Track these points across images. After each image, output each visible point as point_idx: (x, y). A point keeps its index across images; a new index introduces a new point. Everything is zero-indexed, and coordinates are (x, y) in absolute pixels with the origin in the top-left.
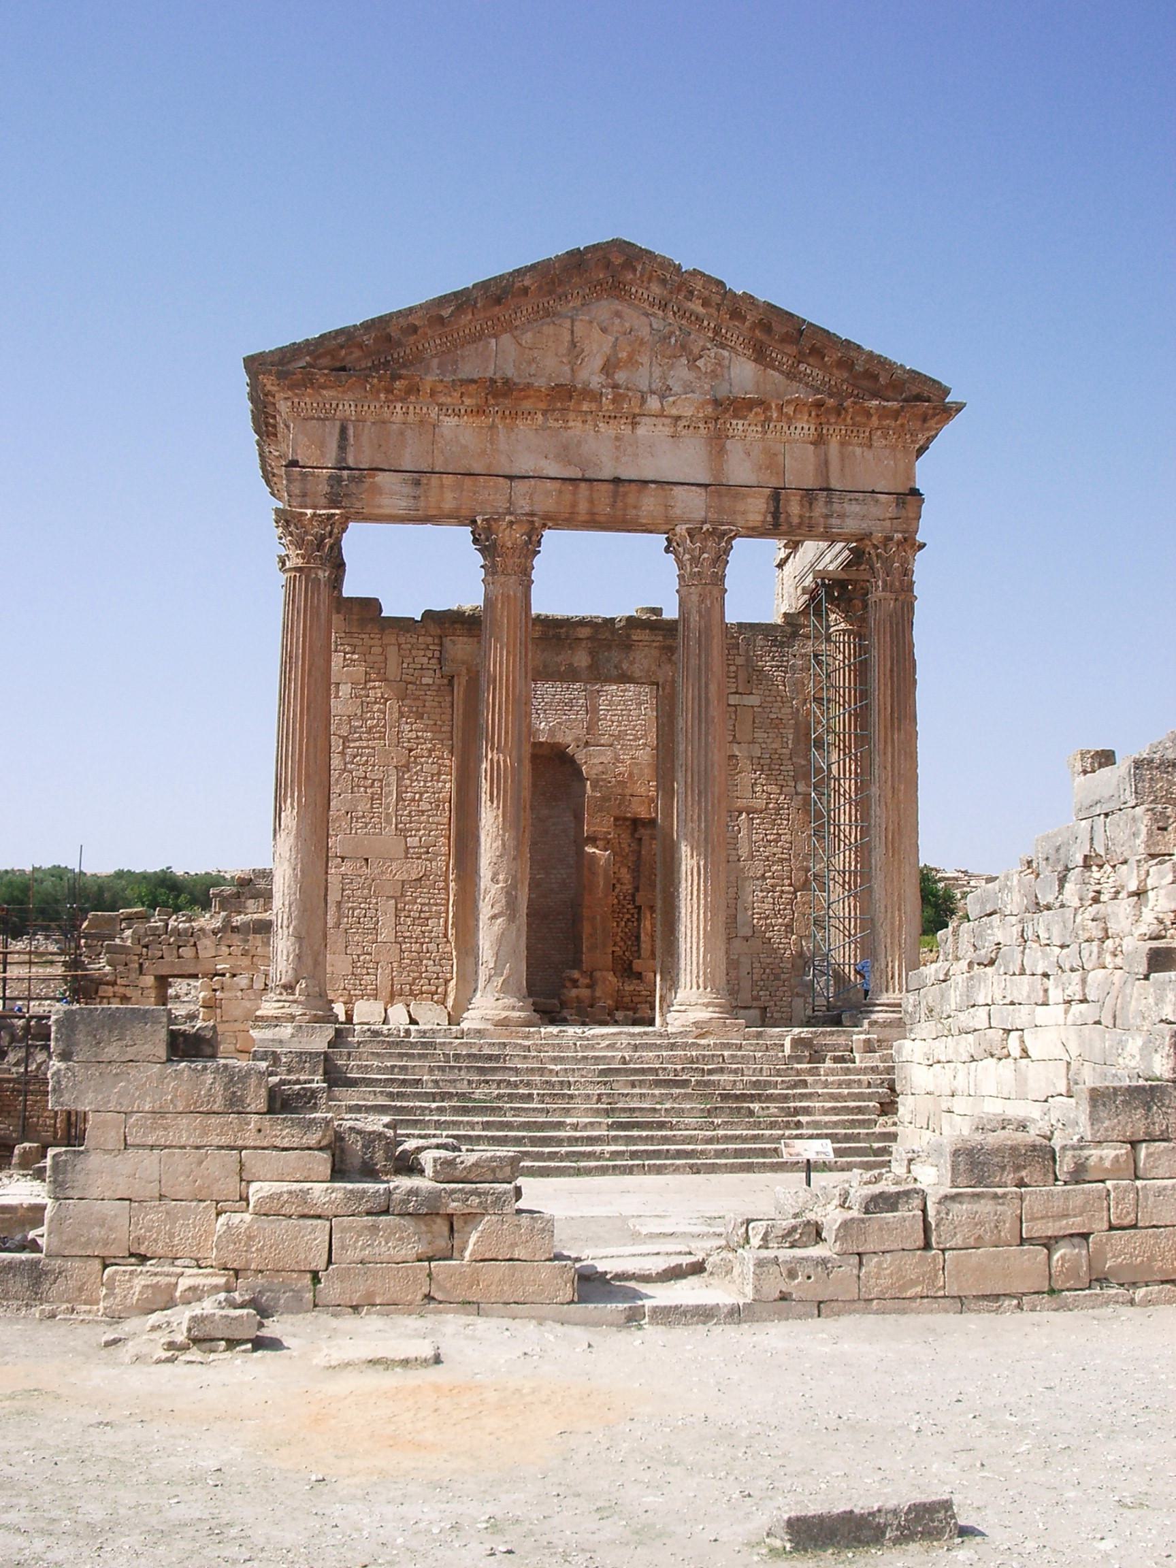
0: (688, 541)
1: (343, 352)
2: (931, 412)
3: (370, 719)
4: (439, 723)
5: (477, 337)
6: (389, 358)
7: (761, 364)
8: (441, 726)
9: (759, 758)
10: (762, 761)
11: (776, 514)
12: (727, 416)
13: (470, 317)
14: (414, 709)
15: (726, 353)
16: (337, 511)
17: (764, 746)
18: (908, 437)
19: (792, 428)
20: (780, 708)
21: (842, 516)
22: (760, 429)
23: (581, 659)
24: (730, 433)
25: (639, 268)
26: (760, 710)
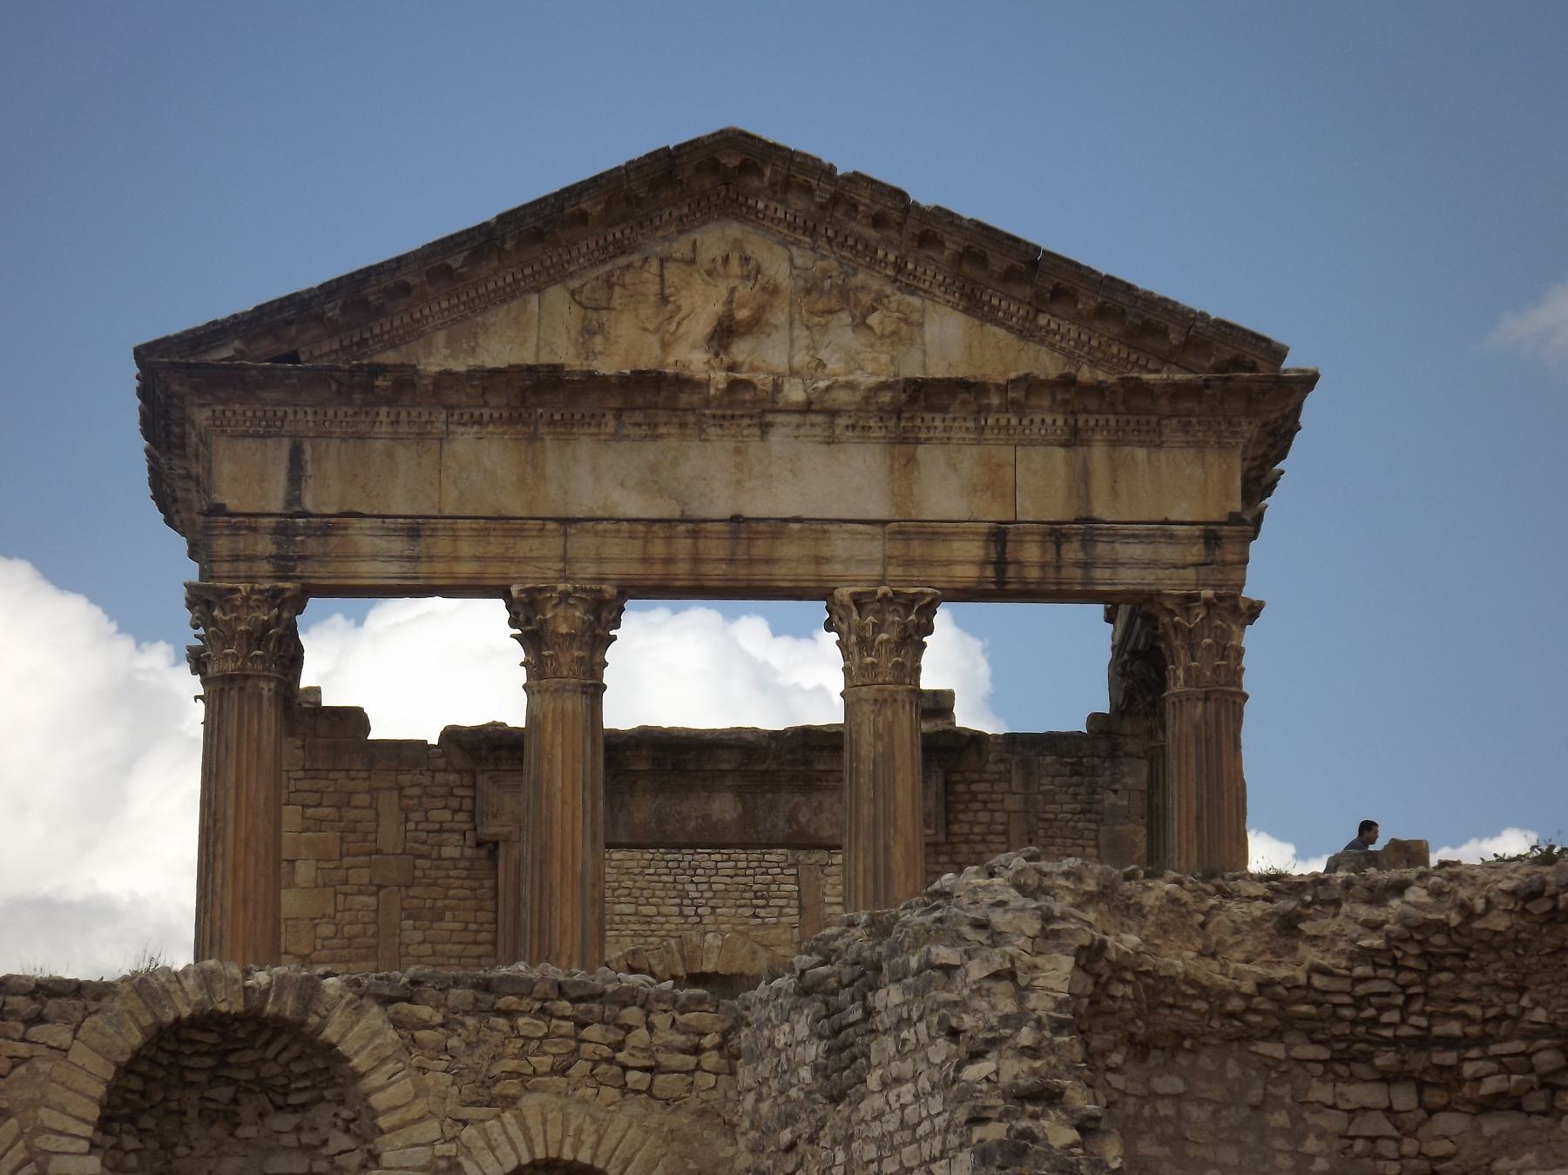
0: (855, 616)
1: (293, 331)
3: (351, 923)
4: (472, 927)
5: (506, 295)
6: (367, 335)
7: (974, 315)
8: (477, 932)
11: (1001, 564)
13: (495, 263)
14: (429, 903)
15: (915, 301)
16: (288, 585)
18: (1223, 428)
19: (1026, 422)
21: (1114, 564)
22: (971, 424)
24: (923, 435)
25: (768, 172)
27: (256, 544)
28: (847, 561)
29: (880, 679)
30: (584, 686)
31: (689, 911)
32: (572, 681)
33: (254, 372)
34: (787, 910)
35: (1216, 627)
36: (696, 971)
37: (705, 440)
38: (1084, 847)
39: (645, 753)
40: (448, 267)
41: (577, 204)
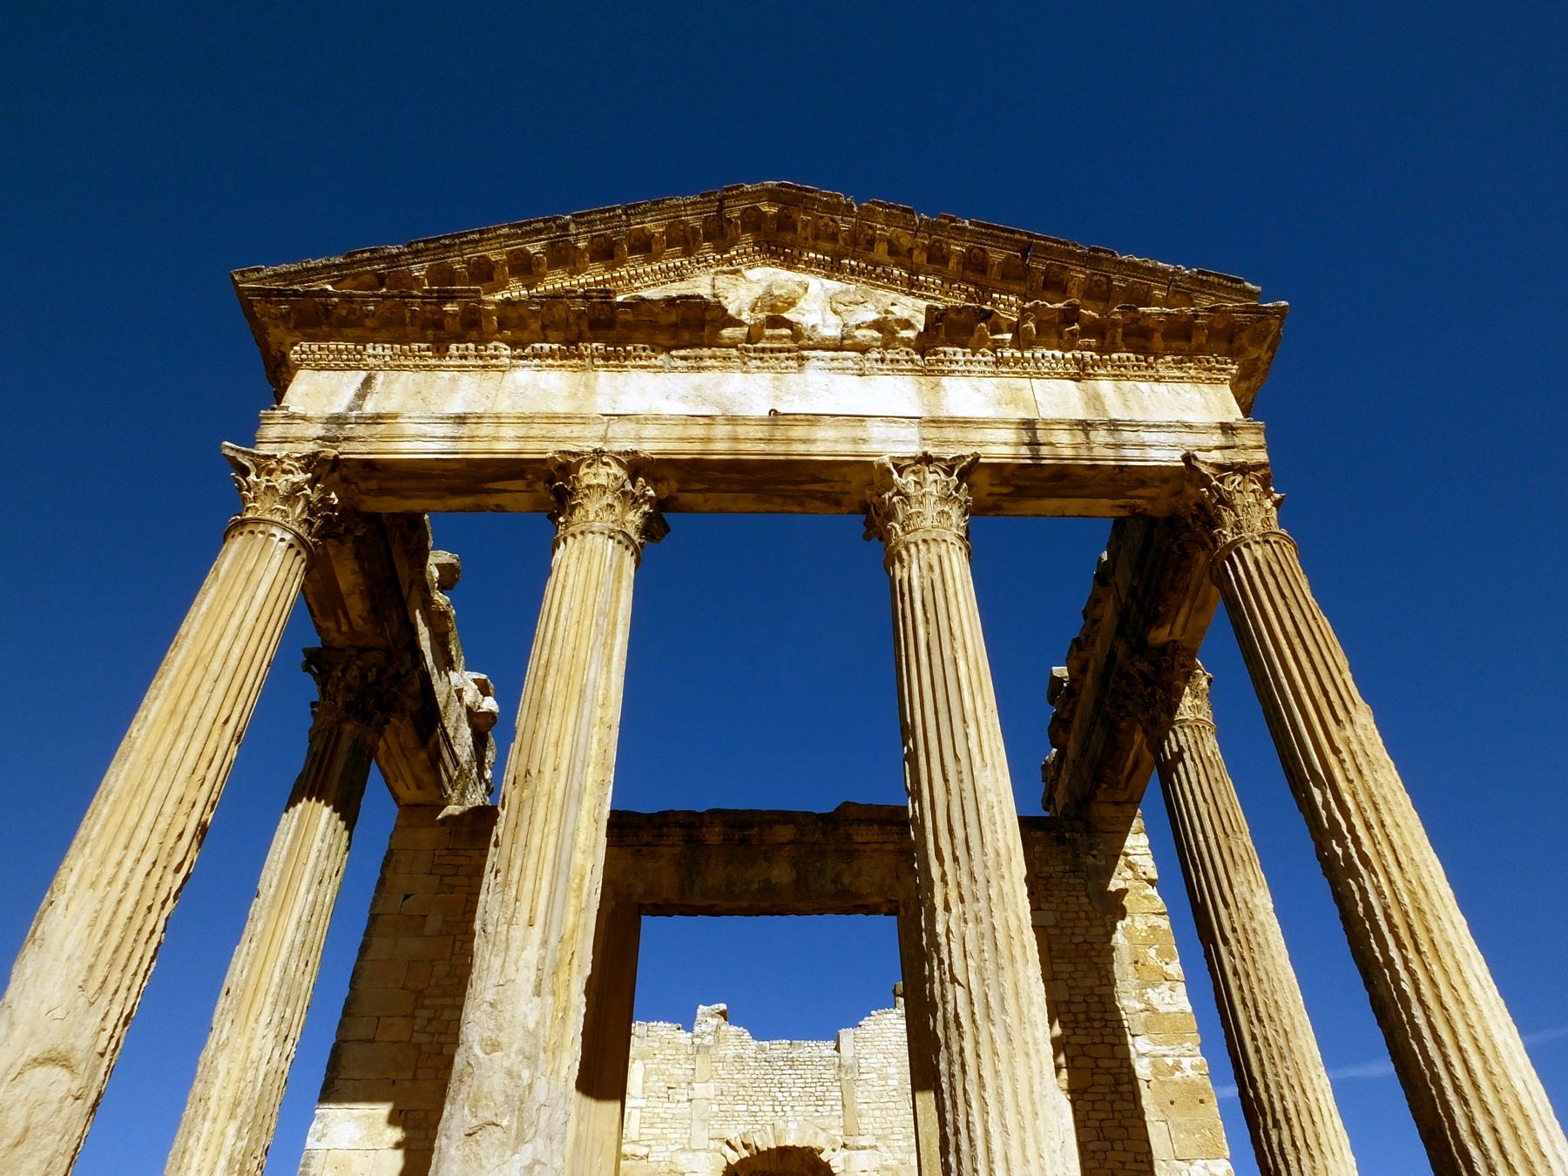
0: (896, 476)
1: (384, 290)
9: (1068, 1003)
10: (1074, 1008)
11: (1034, 444)
17: (1071, 983)
20: (1087, 928)
23: (782, 874)
26: (1057, 931)
27: (307, 429)
28: (884, 441)
29: (928, 524)
30: (612, 530)
31: (778, 1109)
32: (598, 524)
33: (336, 300)
34: (835, 1108)
36: (782, 1145)
37: (745, 372)
38: (1077, 897)
39: (717, 829)
40: (528, 252)
41: (643, 223)
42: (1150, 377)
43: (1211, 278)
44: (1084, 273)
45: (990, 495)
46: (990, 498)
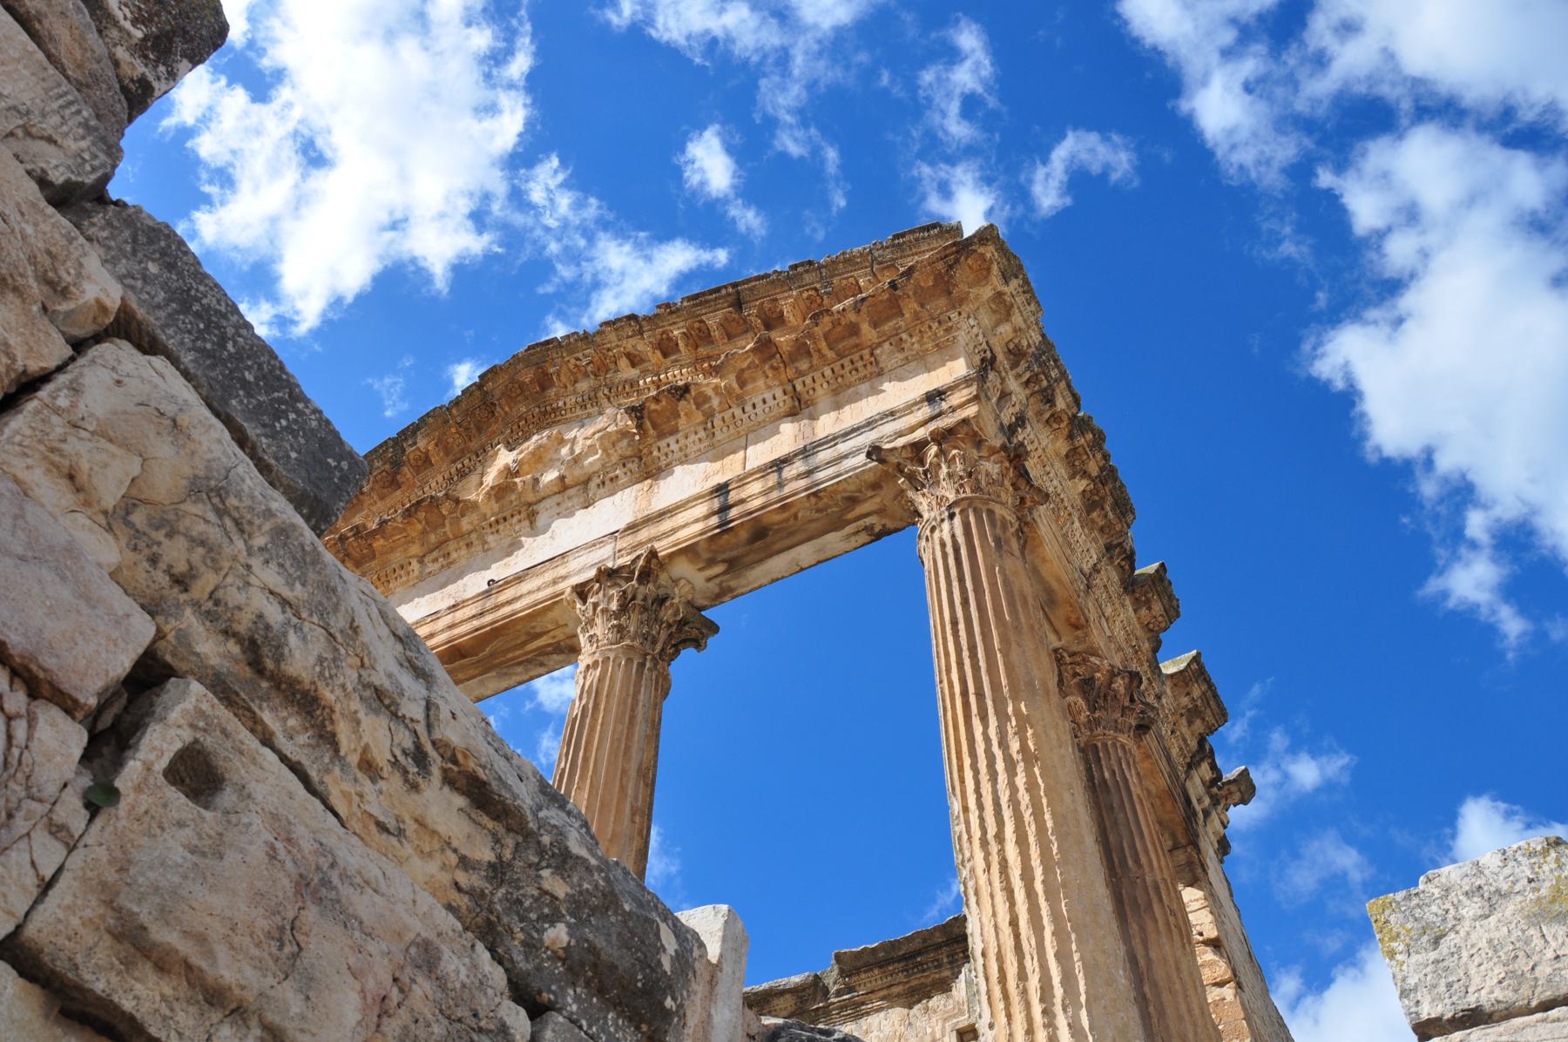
2: (940, 266)
11: (725, 509)
12: (650, 440)
19: (748, 408)
22: (702, 434)
24: (663, 463)
35: (954, 456)
41: (415, 443)
42: (871, 374)
43: (907, 238)
44: (790, 297)
45: (709, 580)
46: (711, 585)
